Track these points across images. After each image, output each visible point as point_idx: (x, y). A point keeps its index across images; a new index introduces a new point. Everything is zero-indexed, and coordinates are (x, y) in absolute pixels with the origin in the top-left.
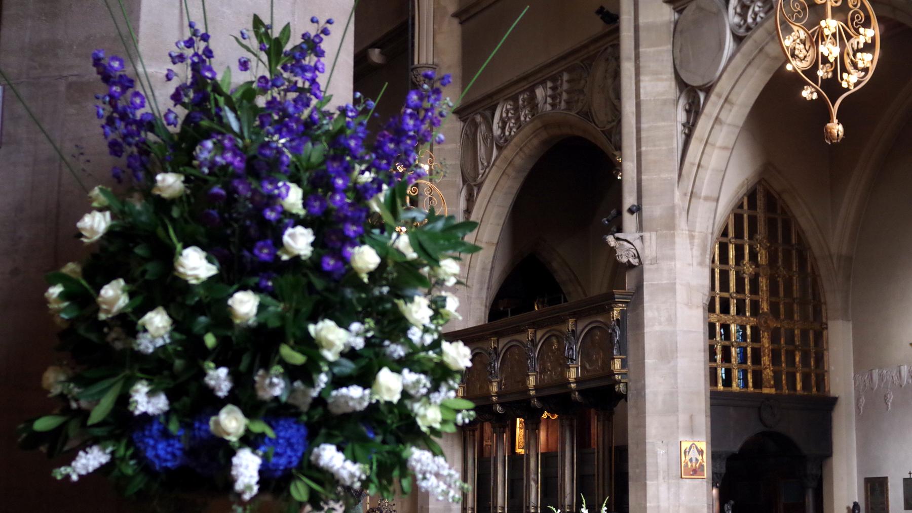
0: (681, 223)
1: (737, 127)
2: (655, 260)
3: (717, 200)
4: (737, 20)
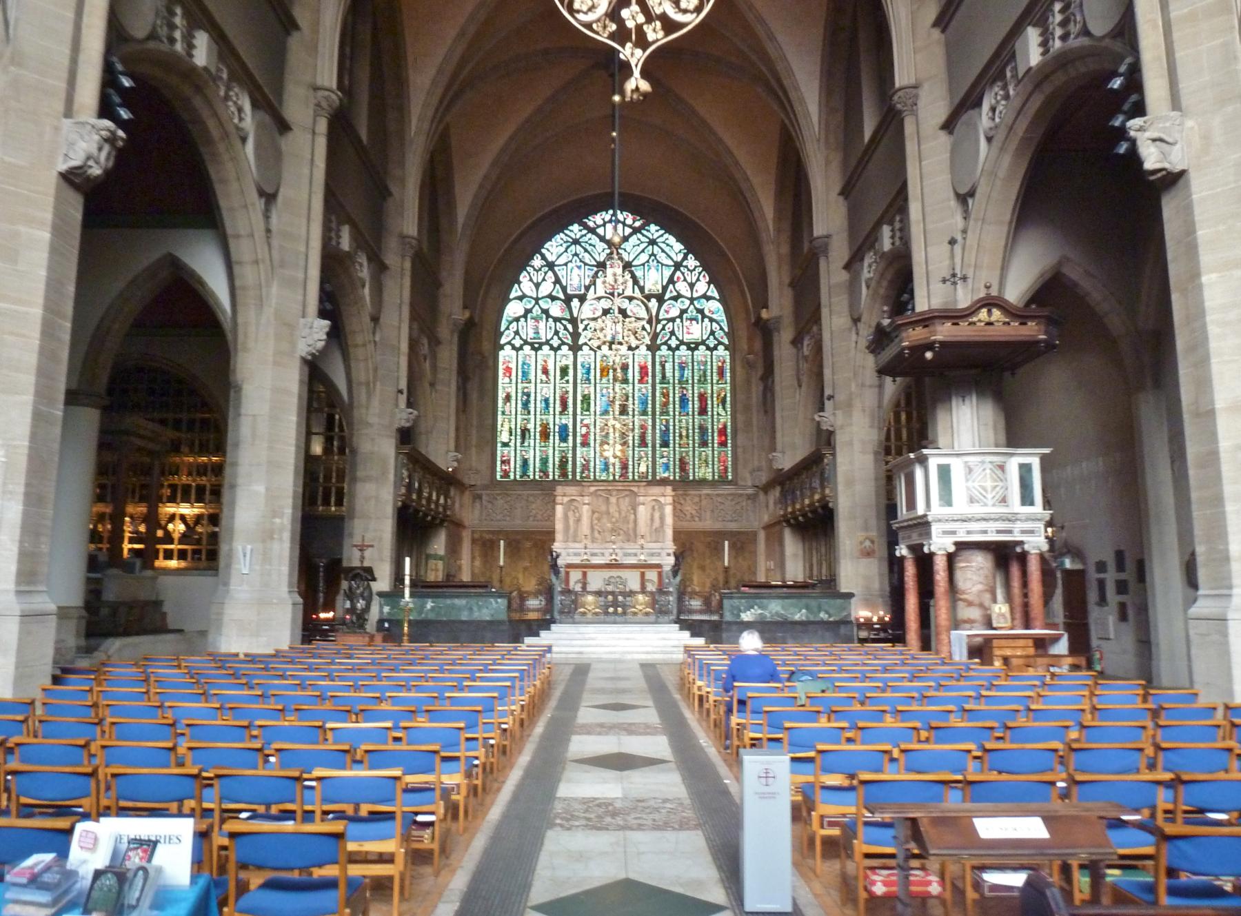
0: (857, 403)
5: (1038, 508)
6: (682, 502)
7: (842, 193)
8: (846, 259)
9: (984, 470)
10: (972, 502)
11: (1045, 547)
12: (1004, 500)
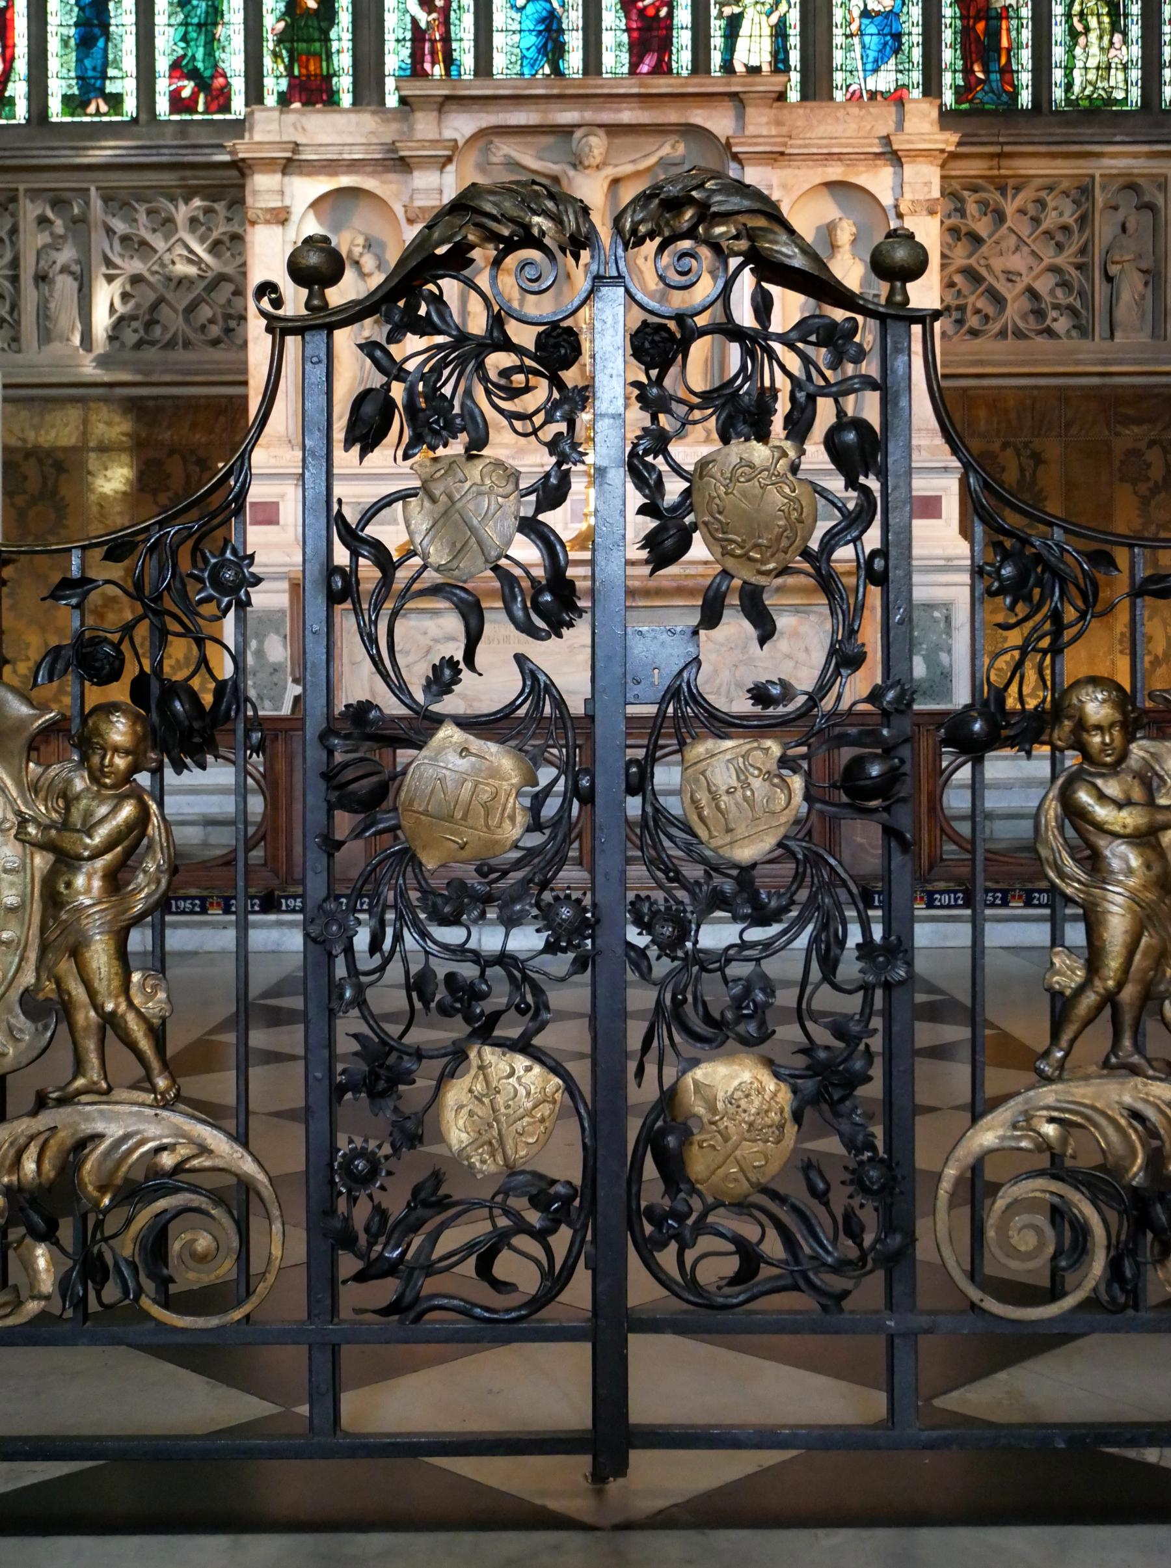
6: (982, 227)
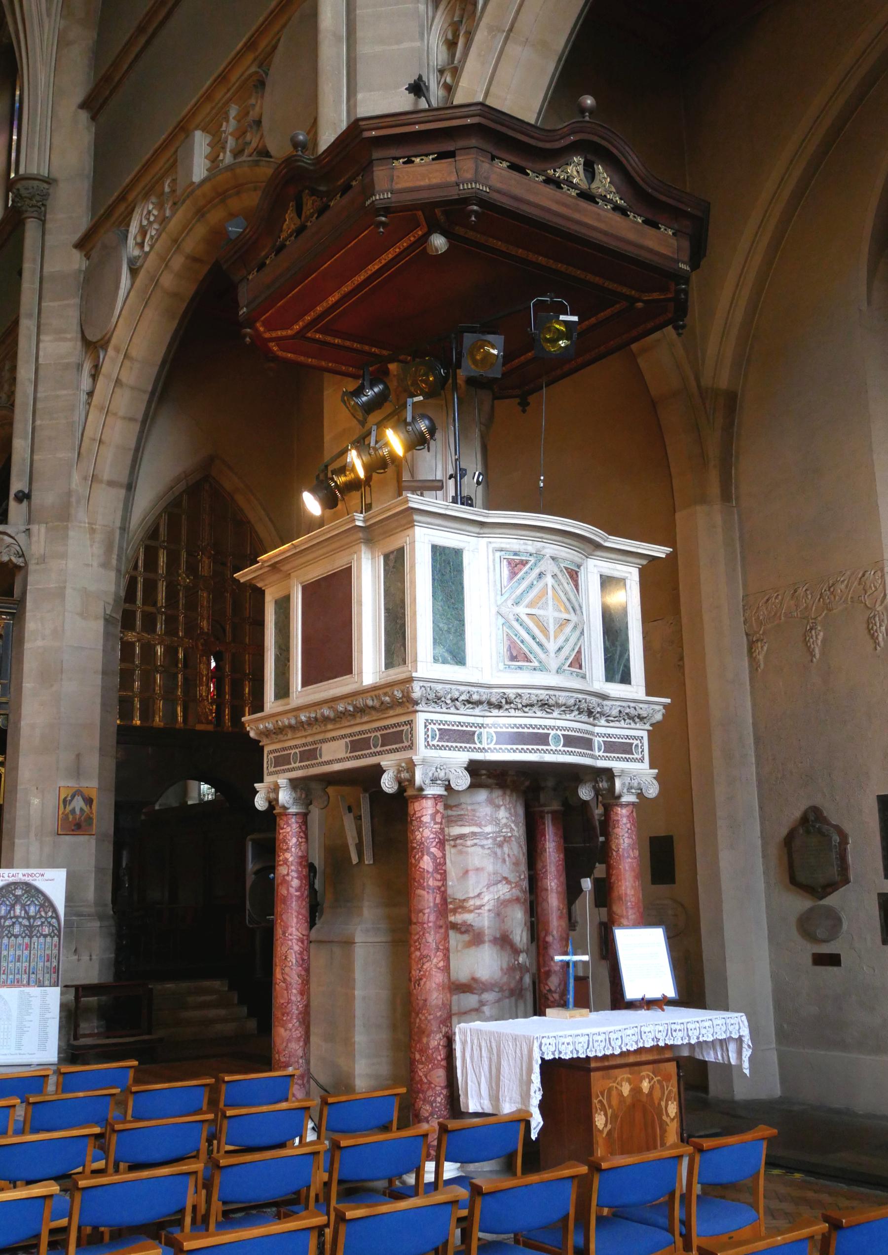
0: (81, 515)
1: (145, 392)
2: (43, 559)
3: (130, 487)
4: (137, 252)
5: (636, 689)
7: (85, 105)
8: (84, 223)
9: (541, 575)
10: (513, 658)
11: (653, 791)
12: (577, 662)
